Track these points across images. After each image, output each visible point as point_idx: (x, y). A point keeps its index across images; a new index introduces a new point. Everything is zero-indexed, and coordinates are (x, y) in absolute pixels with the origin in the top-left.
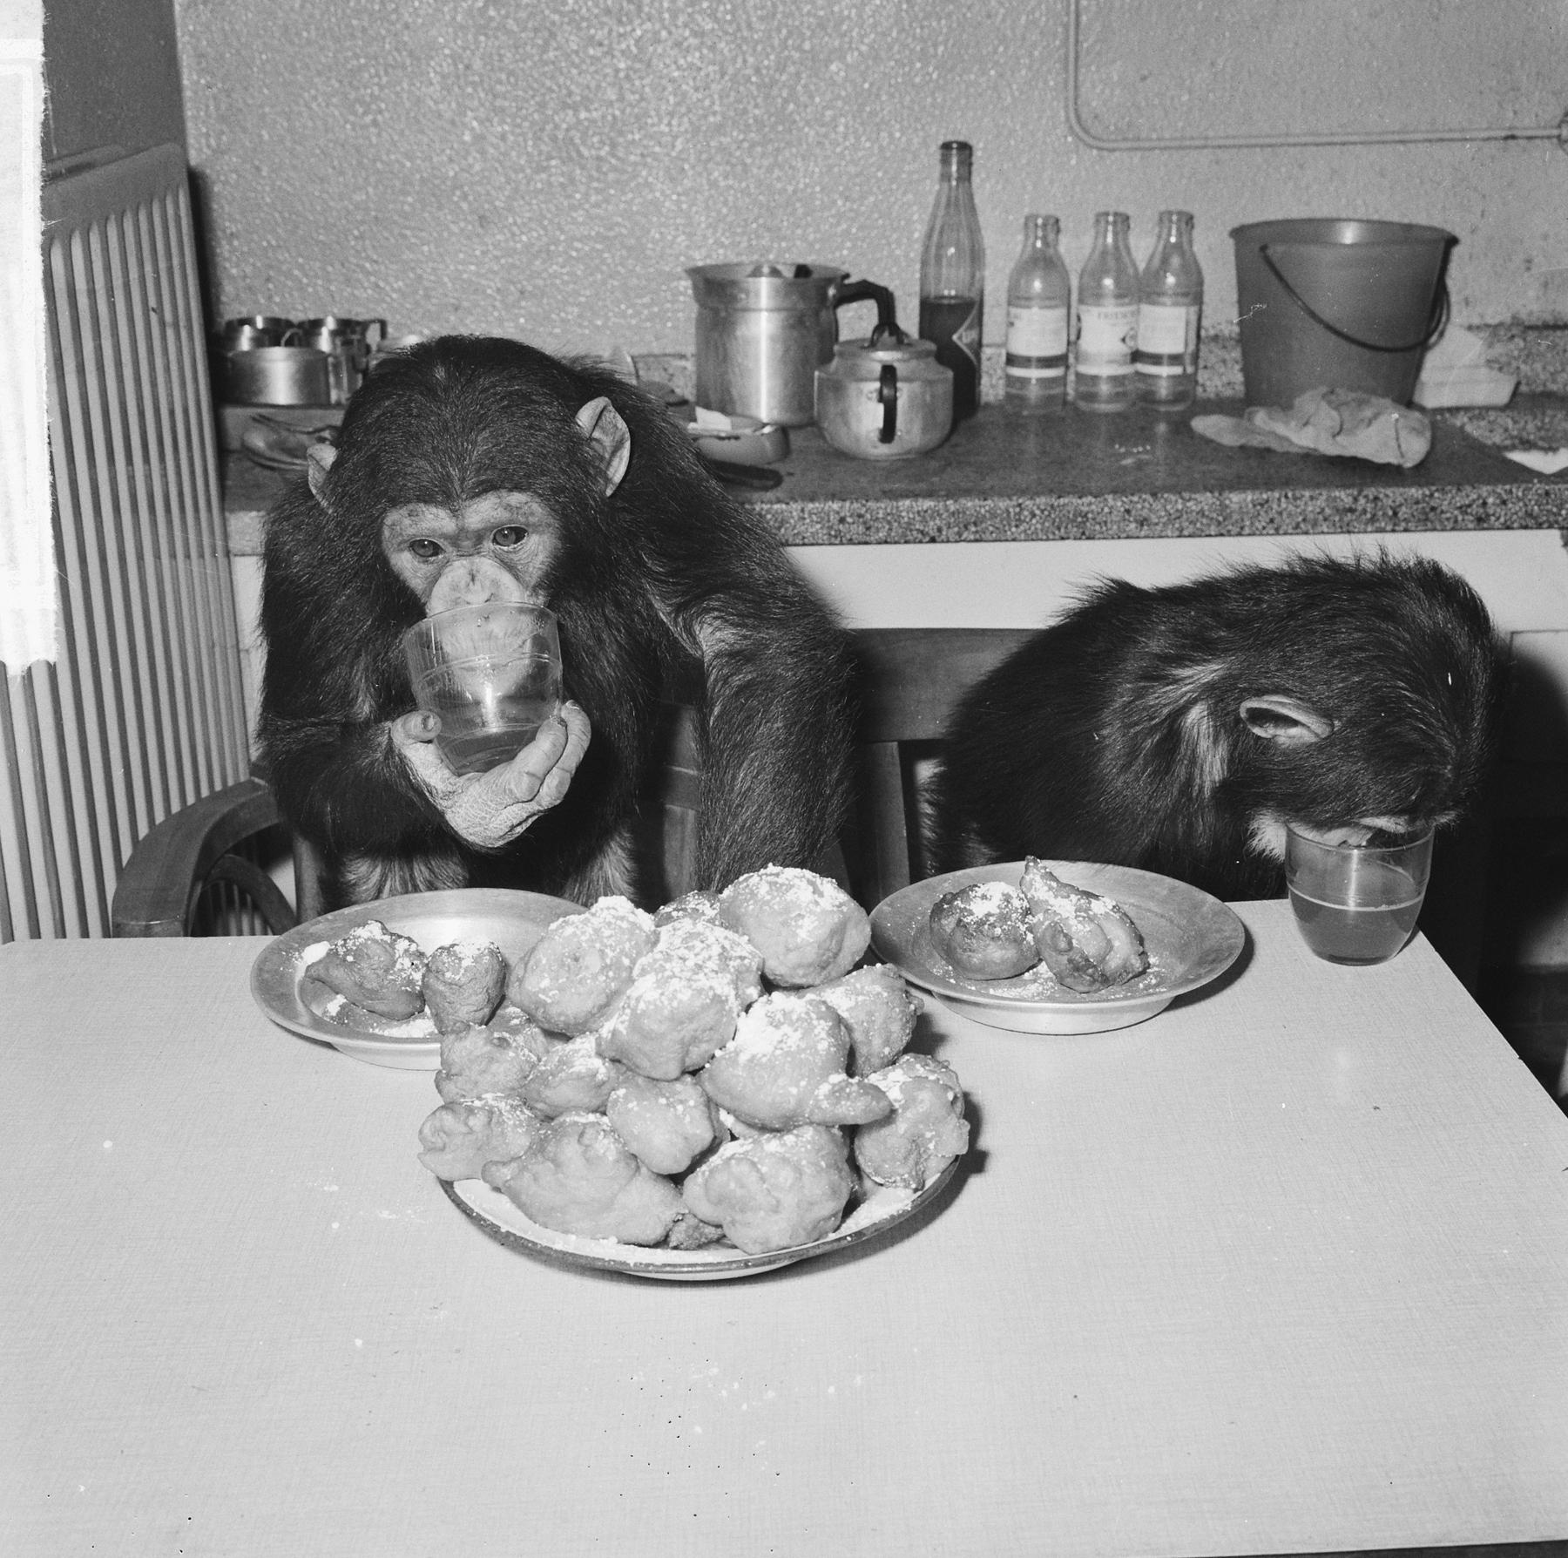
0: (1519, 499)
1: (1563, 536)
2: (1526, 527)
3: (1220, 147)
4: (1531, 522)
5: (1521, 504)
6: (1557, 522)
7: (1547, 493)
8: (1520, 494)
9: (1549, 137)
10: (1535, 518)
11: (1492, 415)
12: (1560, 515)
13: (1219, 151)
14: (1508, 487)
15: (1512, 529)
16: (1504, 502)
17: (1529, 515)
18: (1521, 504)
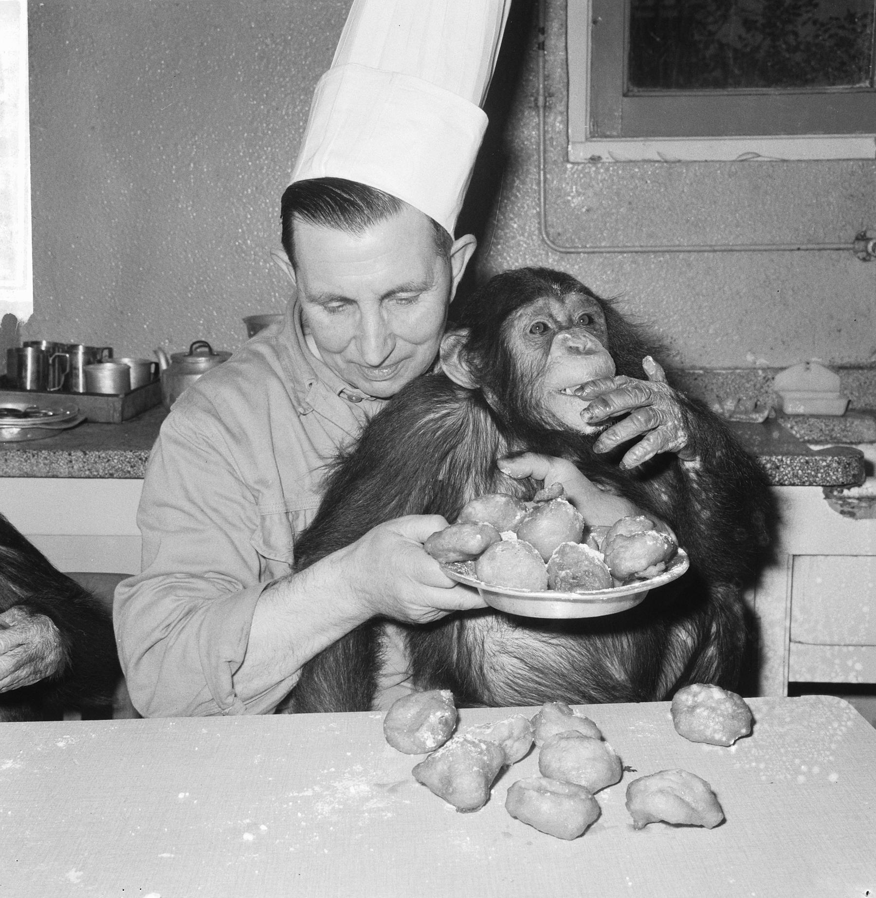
0: (788, 466)
1: (824, 492)
2: (794, 485)
3: (636, 252)
4: (797, 481)
5: (789, 469)
6: (815, 482)
7: (807, 462)
8: (788, 462)
9: (848, 249)
10: (800, 478)
11: (812, 420)
12: (817, 477)
13: (636, 256)
14: (780, 457)
15: (785, 485)
16: (778, 468)
17: (795, 476)
18: (789, 469)
